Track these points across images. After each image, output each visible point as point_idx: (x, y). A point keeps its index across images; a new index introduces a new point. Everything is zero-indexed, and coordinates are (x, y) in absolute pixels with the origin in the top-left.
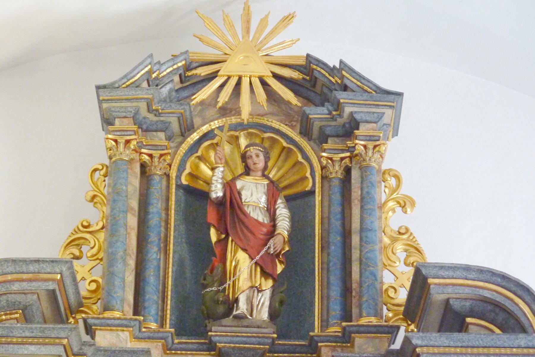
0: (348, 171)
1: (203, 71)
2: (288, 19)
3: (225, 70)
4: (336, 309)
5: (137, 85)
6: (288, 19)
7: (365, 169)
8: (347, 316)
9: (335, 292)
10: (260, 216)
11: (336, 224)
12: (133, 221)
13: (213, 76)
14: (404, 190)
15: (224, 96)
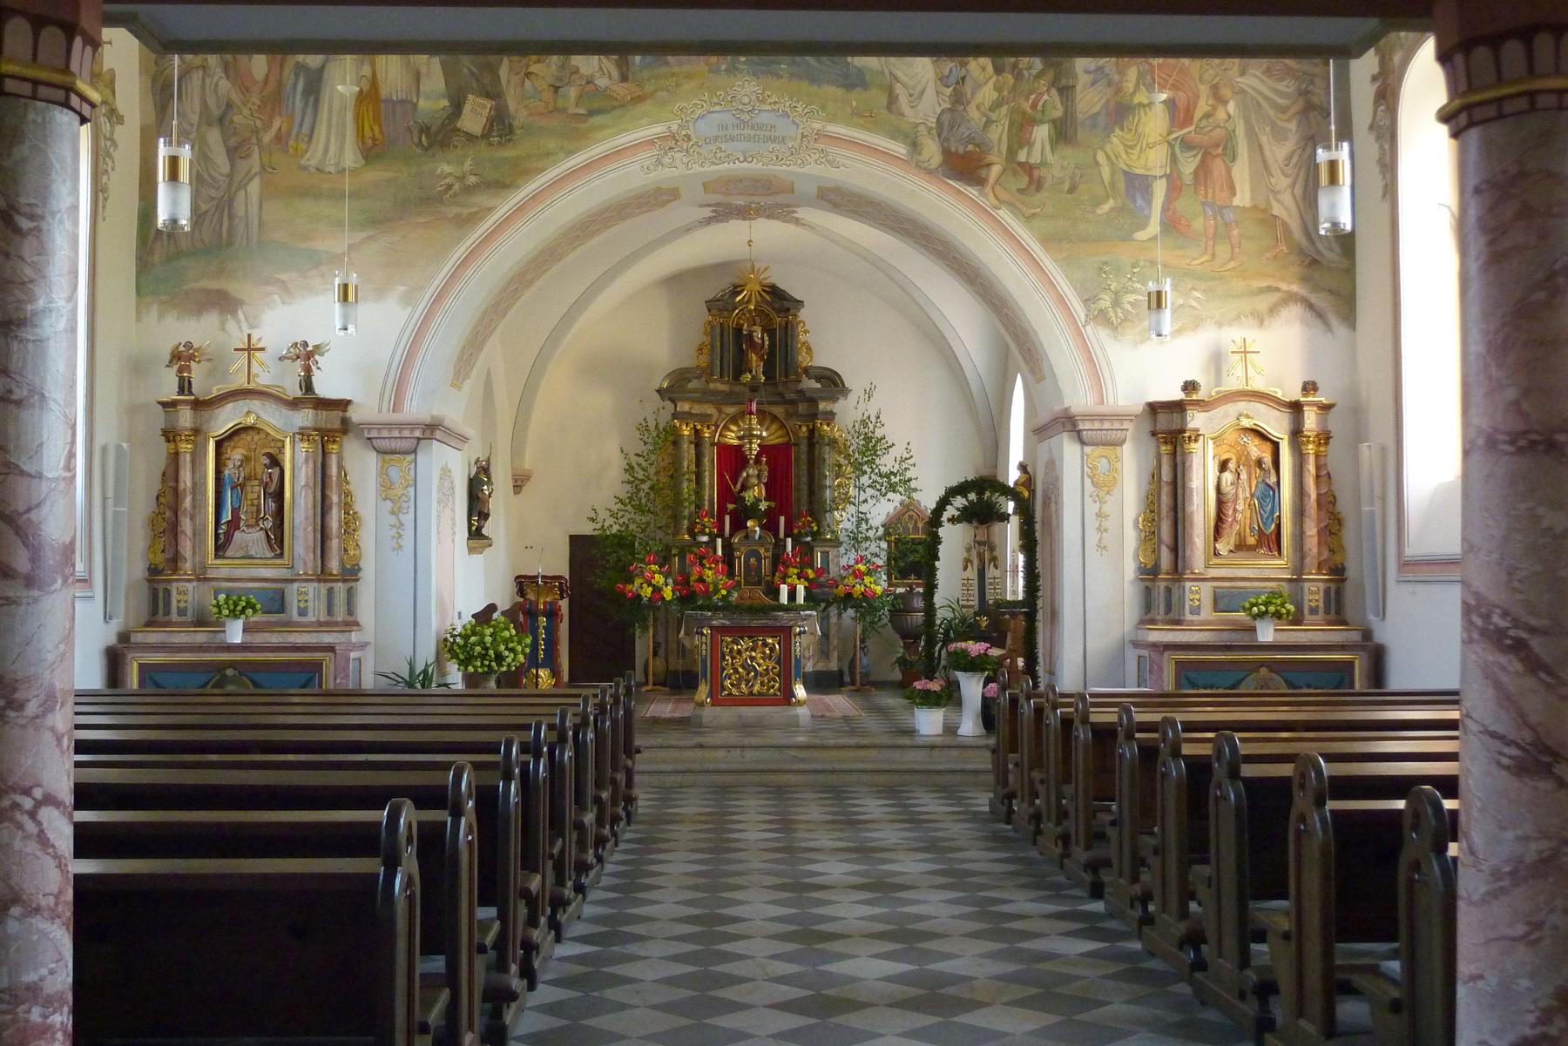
0: (787, 324)
1: (739, 289)
2: (766, 269)
3: (748, 287)
4: (783, 373)
5: (718, 300)
6: (766, 269)
7: (792, 326)
8: (787, 376)
9: (783, 367)
10: (760, 341)
11: (783, 342)
12: (718, 344)
13: (742, 291)
14: (806, 328)
15: (746, 299)
